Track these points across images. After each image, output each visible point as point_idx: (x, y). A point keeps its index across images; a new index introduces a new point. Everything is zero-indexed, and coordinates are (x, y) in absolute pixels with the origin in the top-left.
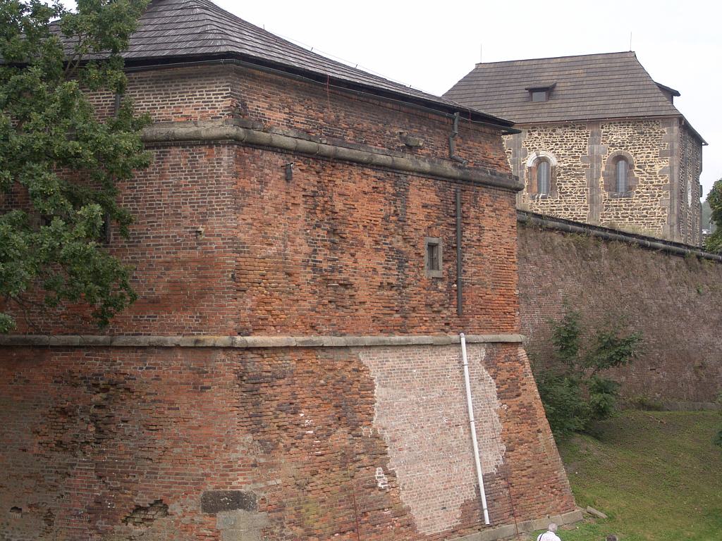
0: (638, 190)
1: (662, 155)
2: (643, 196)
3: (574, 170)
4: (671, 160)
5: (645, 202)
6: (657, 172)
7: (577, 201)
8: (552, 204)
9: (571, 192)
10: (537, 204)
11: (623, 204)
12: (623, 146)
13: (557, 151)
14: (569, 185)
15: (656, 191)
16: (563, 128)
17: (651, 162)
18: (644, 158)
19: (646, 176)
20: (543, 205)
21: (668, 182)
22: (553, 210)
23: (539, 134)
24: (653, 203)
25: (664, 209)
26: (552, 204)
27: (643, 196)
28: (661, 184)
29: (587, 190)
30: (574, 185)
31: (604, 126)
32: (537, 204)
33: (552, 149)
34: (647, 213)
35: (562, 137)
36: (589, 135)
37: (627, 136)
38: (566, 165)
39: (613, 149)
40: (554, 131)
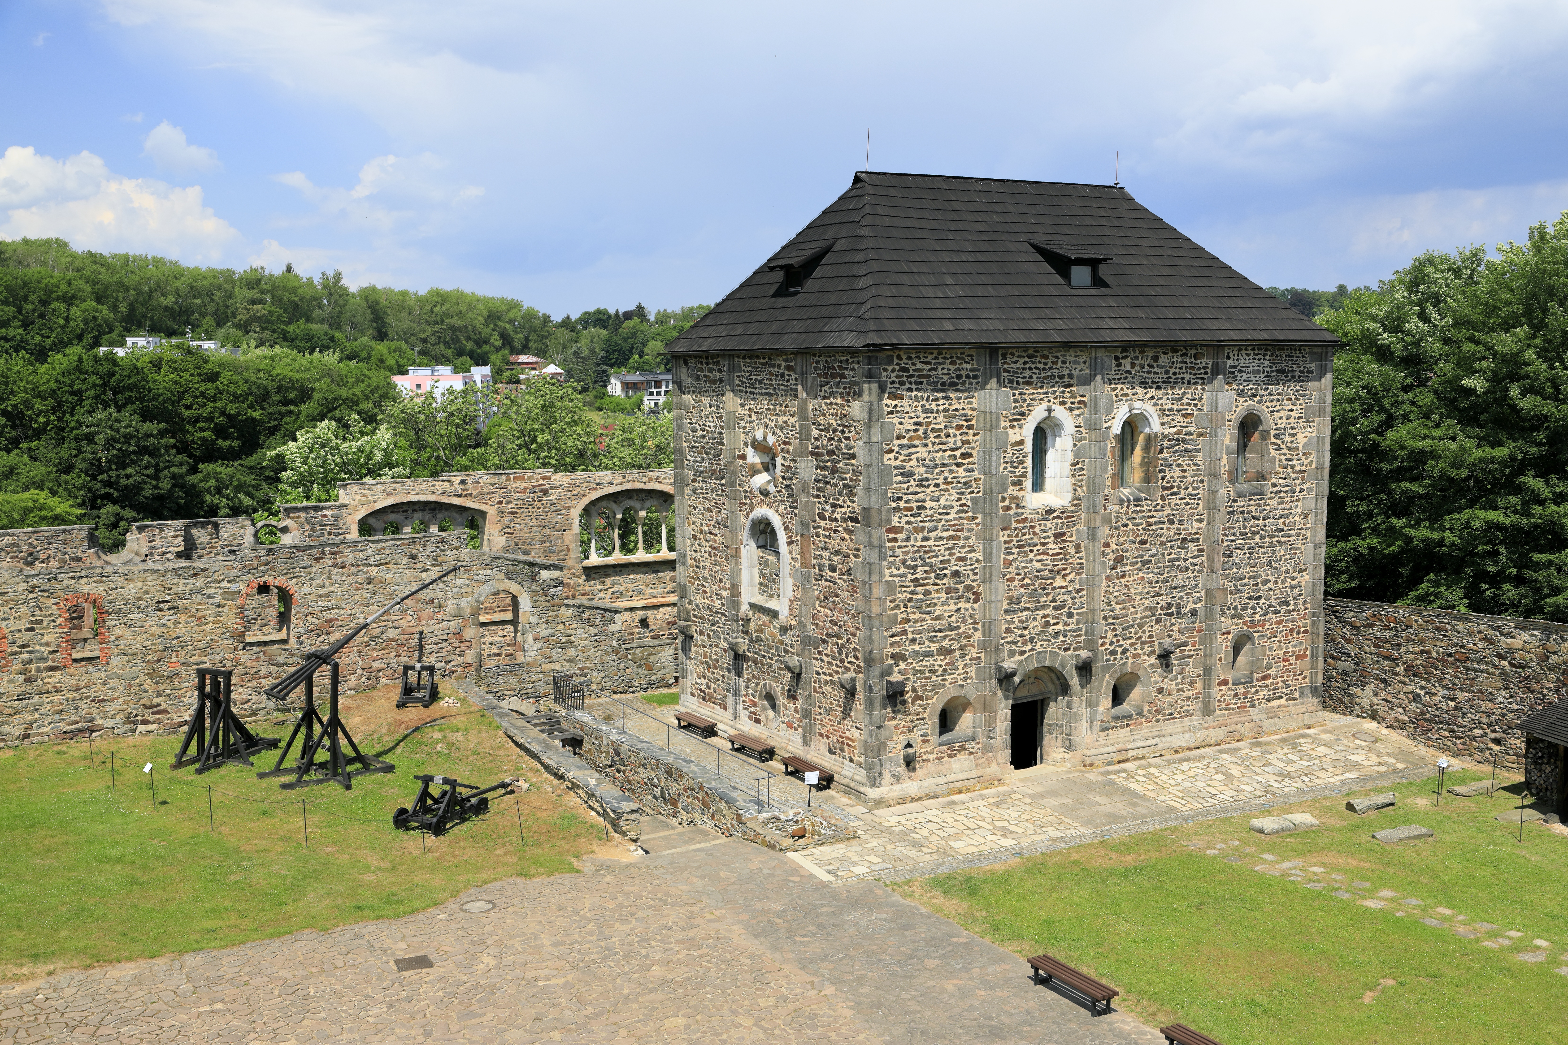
0: (1274, 480)
1: (1306, 418)
2: (1280, 492)
3: (1183, 441)
4: (1319, 424)
5: (1282, 503)
6: (1300, 446)
7: (1187, 504)
8: (1150, 511)
9: (1179, 487)
10: (1127, 513)
11: (1253, 508)
12: (1255, 396)
13: (1159, 402)
14: (1177, 472)
15: (1297, 482)
16: (1170, 354)
17: (1293, 428)
18: (1284, 420)
19: (1285, 455)
20: (1134, 515)
21: (1314, 466)
22: (1150, 525)
23: (1133, 365)
24: (1293, 505)
25: (1306, 516)
26: (1150, 511)
27: (1280, 492)
28: (1303, 468)
29: (1202, 481)
30: (1184, 471)
31: (1231, 355)
32: (1127, 513)
33: (1153, 397)
34: (1284, 523)
35: (1167, 372)
36: (1209, 370)
37: (1262, 375)
38: (1173, 430)
39: (1242, 400)
40: (1155, 359)
